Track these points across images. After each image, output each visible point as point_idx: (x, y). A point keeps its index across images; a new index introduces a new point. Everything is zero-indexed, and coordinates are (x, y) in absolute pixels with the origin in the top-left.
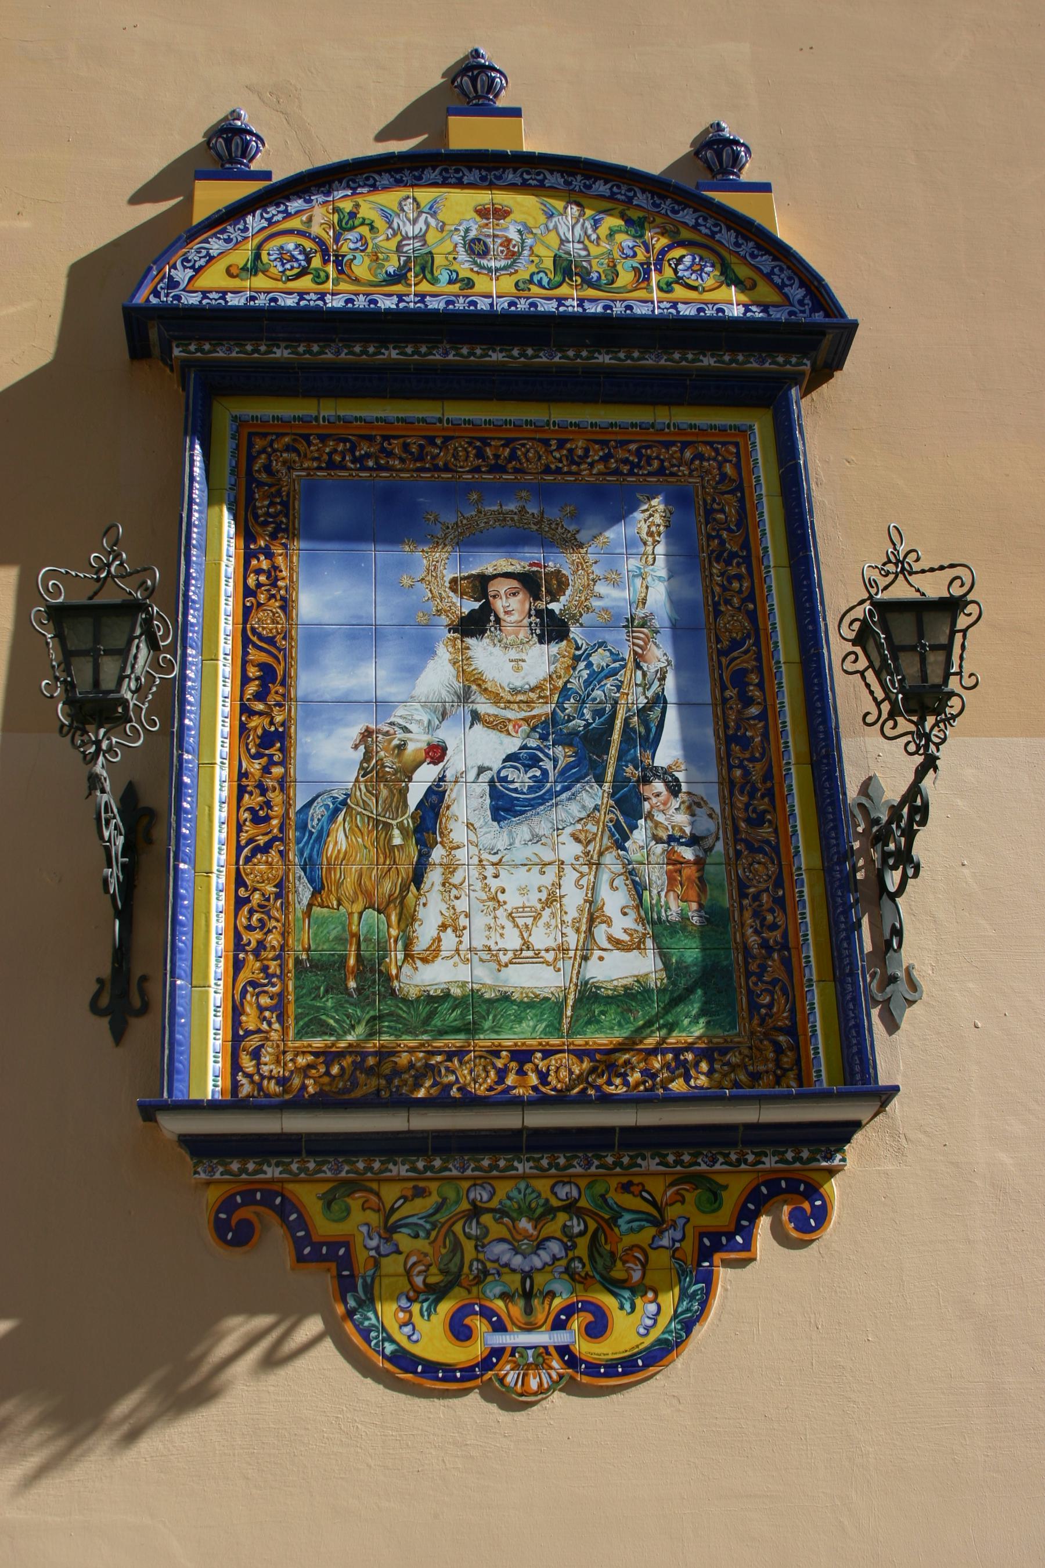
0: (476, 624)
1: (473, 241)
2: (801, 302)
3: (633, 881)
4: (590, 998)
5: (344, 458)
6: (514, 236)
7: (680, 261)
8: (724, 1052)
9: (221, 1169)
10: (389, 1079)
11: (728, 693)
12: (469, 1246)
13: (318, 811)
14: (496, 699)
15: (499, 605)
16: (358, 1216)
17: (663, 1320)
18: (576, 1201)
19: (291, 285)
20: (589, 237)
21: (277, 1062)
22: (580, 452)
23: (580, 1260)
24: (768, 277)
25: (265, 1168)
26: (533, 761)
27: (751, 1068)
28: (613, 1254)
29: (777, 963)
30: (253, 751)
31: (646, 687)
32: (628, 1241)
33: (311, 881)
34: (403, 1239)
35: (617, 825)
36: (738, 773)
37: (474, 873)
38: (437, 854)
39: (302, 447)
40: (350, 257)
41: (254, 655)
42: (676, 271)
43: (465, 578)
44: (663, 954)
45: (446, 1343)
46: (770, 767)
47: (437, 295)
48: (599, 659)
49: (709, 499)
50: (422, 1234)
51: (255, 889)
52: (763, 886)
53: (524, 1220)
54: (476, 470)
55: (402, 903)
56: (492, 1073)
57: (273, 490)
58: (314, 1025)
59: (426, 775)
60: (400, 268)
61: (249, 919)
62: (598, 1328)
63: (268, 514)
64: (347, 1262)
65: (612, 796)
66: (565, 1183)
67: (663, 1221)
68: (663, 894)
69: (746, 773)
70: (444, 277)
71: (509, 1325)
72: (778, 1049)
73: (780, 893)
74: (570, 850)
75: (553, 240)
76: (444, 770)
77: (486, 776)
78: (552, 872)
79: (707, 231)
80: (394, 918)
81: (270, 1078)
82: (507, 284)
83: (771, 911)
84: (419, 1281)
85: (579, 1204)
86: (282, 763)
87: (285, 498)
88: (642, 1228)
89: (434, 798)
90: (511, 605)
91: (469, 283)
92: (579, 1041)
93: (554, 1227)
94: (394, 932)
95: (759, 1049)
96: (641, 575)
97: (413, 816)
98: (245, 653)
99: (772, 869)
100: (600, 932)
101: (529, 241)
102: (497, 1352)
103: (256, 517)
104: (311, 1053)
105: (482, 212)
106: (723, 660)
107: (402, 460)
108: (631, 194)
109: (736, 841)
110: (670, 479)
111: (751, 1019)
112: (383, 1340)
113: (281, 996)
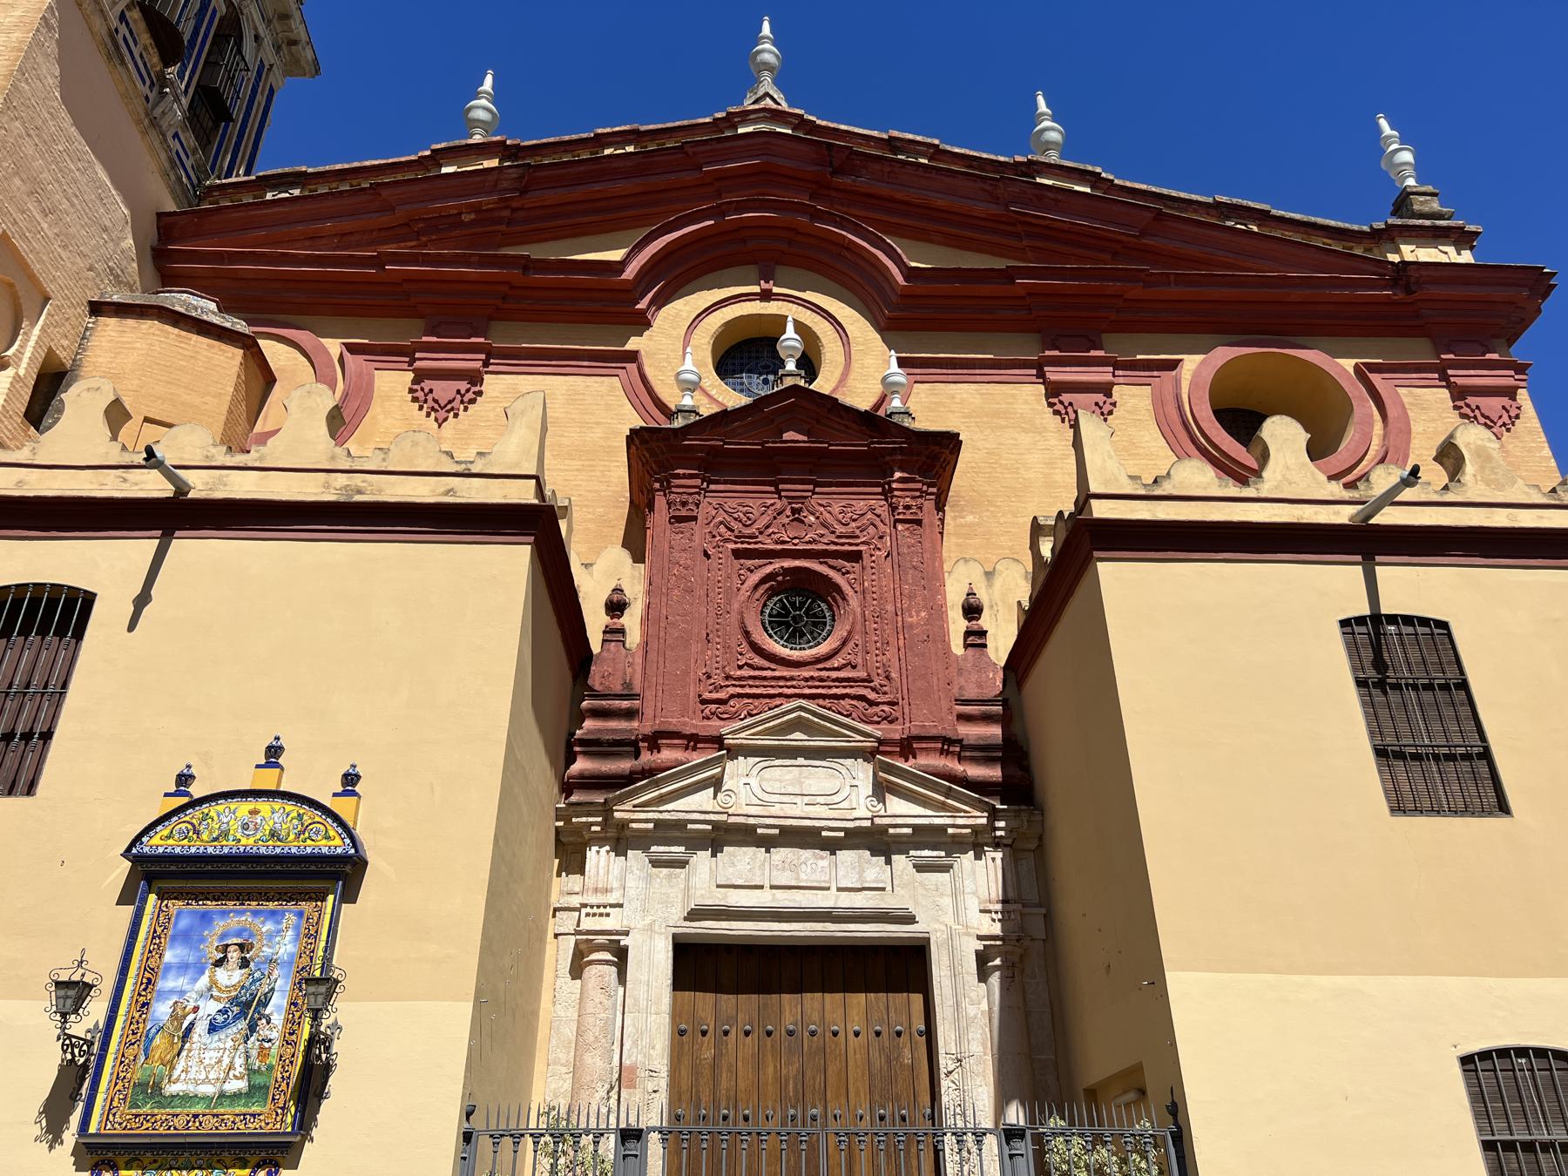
0: (219, 963)
4: (222, 1095)
14: (220, 990)
47: (227, 847)
59: (191, 1017)
82: (251, 841)
90: (234, 955)
105: (251, 813)
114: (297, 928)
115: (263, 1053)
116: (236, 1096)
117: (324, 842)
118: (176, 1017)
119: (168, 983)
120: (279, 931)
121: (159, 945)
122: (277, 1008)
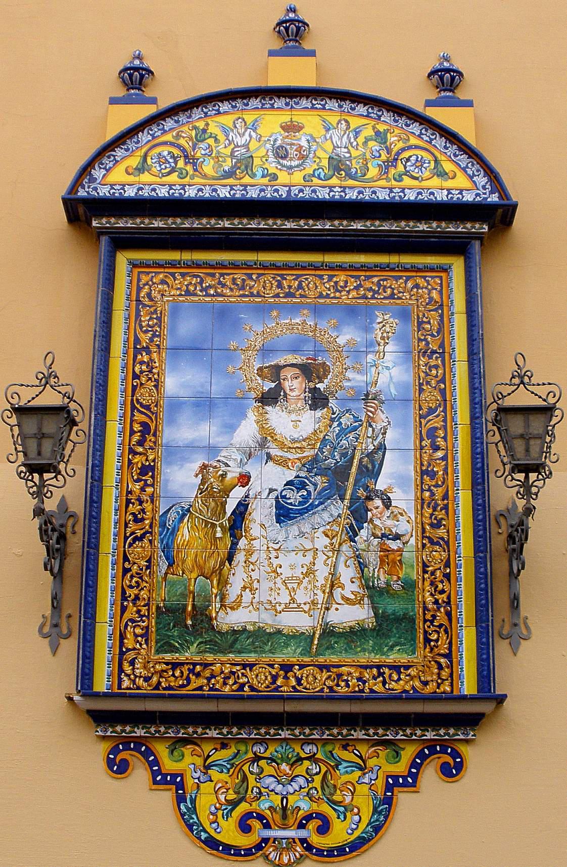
1: (278, 148)
2: (484, 187)
3: (359, 562)
4: (328, 632)
5: (196, 289)
6: (304, 143)
7: (408, 160)
8: (407, 667)
9: (111, 730)
10: (209, 679)
11: (424, 443)
12: (251, 779)
13: (172, 515)
14: (282, 446)
15: (287, 385)
16: (188, 759)
17: (362, 826)
18: (315, 754)
19: (164, 179)
20: (351, 144)
21: (145, 667)
22: (342, 284)
23: (316, 789)
24: (464, 170)
25: (136, 730)
26: (302, 486)
27: (423, 678)
28: (335, 786)
29: (443, 615)
30: (135, 477)
31: (374, 438)
32: (345, 778)
33: (167, 559)
34: (214, 773)
35: (351, 526)
36: (427, 494)
37: (263, 555)
38: (242, 543)
39: (170, 280)
40: (201, 160)
41: (138, 417)
42: (405, 167)
43: (266, 367)
44: (375, 609)
45: (236, 833)
46: (447, 491)
48: (346, 420)
49: (421, 315)
50: (225, 771)
51: (135, 563)
52: (438, 566)
53: (284, 764)
54: (277, 296)
55: (220, 573)
56: (269, 677)
57: (152, 310)
58: (166, 646)
59: (238, 493)
60: (232, 167)
61: (131, 581)
62: (324, 828)
63: (148, 325)
64: (181, 786)
65: (349, 508)
66: (309, 744)
68: (376, 570)
69: (432, 494)
70: (259, 173)
71: (273, 825)
72: (440, 667)
73: (448, 571)
74: (322, 542)
75: (329, 146)
76: (249, 490)
77: (273, 495)
78: (310, 555)
79: (427, 139)
80: (215, 582)
81: (141, 677)
83: (442, 582)
84: (222, 798)
86: (152, 485)
88: (353, 771)
89: (242, 508)
90: (294, 385)
91: (275, 177)
92: (321, 660)
93: (301, 769)
94: (215, 591)
95: (429, 667)
96: (375, 365)
97: (229, 520)
98: (133, 415)
99: (444, 555)
100: (337, 593)
101: (314, 148)
102: (266, 840)
103: (141, 327)
104: (164, 663)
106: (422, 420)
107: (231, 290)
108: (380, 113)
109: (423, 537)
110: (398, 301)
111: (425, 648)
112: (201, 831)
113: (147, 627)
114: (402, 338)
115: (390, 560)
116: (354, 635)
117: (436, 182)
118: (213, 491)
119: (180, 432)
120: (370, 344)
121: (150, 365)
122: (397, 475)
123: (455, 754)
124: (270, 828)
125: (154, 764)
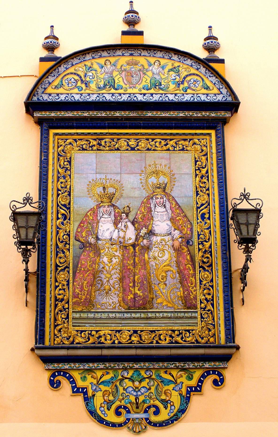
7: (190, 80)
51: (60, 283)
62: (157, 412)
64: (85, 393)
67: (177, 383)
85: (152, 377)
87: (69, 160)
102: (128, 419)
123: (220, 374)
124: (130, 413)
125: (73, 382)
